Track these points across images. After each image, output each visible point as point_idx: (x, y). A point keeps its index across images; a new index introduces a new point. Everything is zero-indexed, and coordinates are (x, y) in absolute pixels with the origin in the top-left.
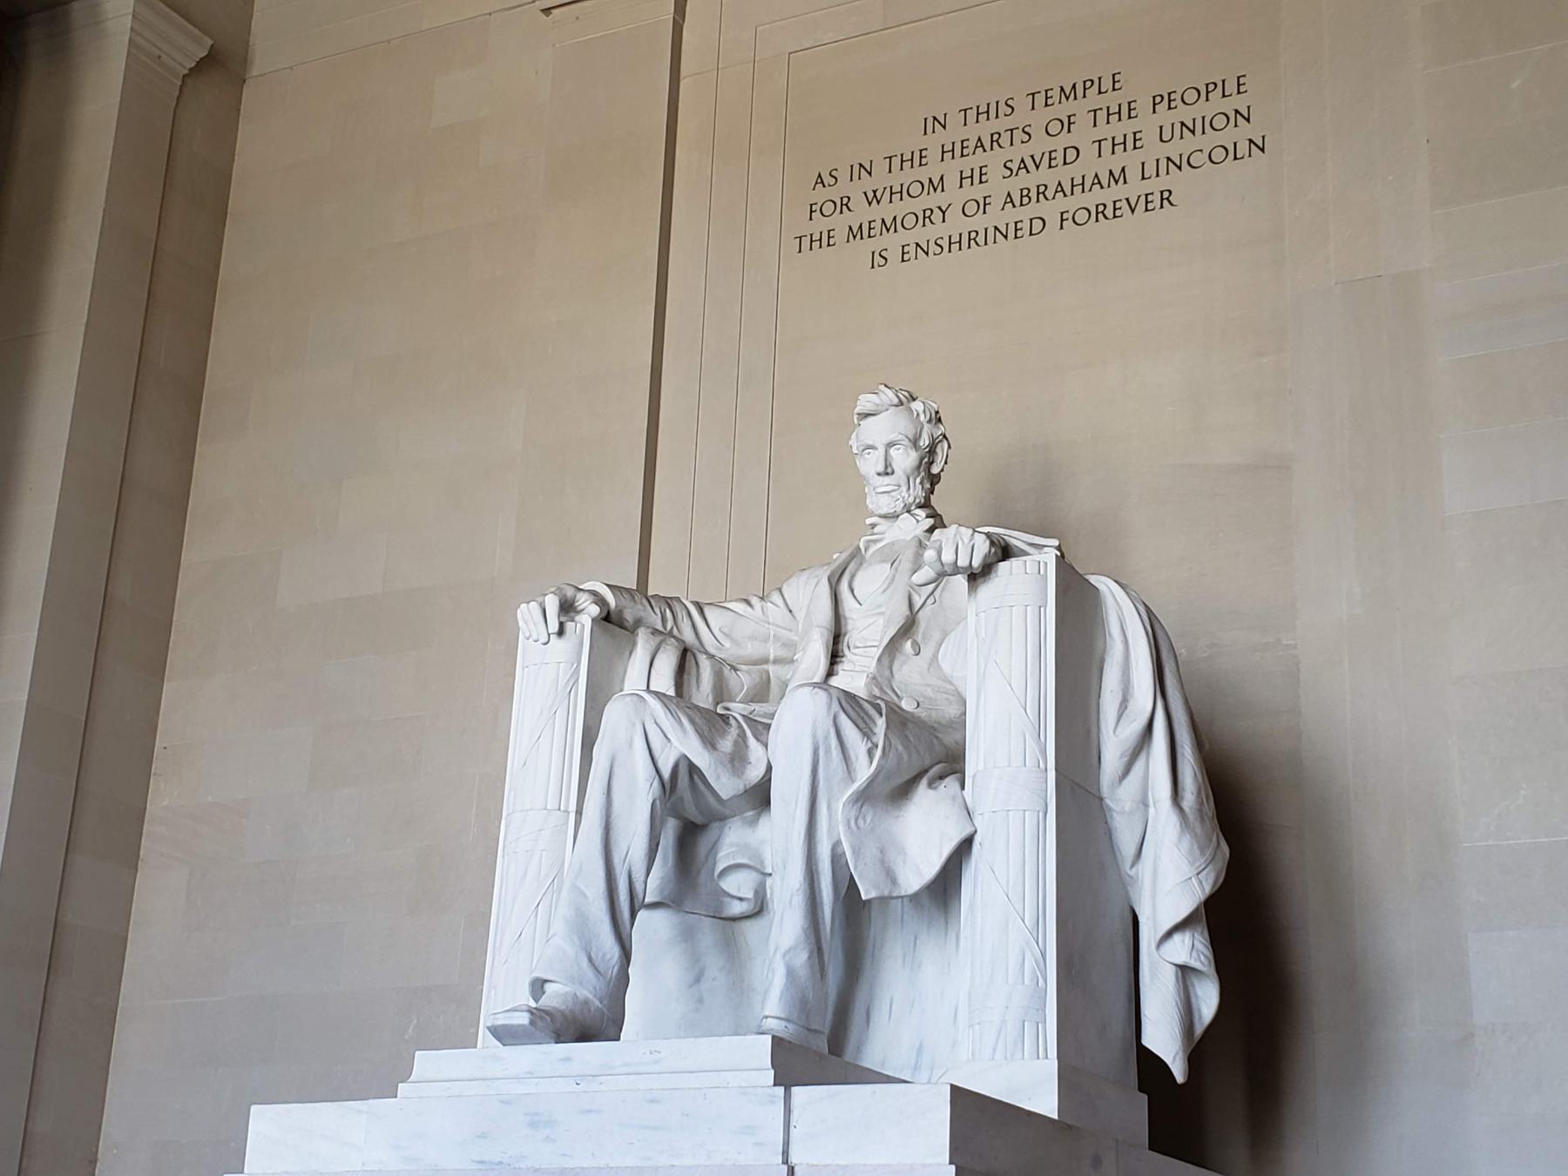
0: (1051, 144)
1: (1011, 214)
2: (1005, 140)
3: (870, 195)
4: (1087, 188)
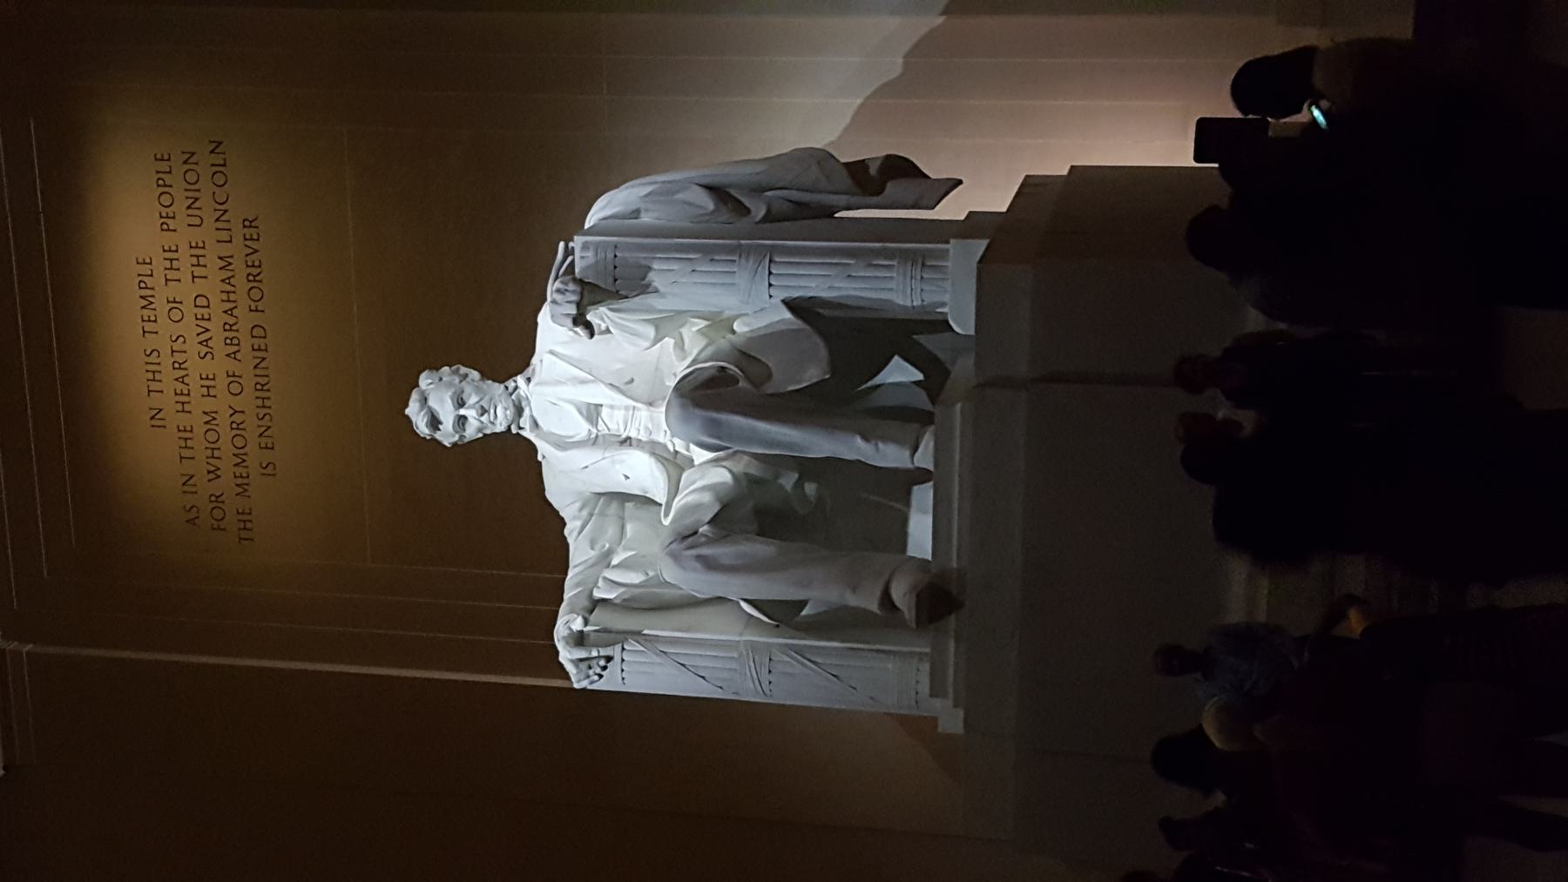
0: (189, 318)
2: (179, 358)
3: (212, 476)
4: (229, 288)
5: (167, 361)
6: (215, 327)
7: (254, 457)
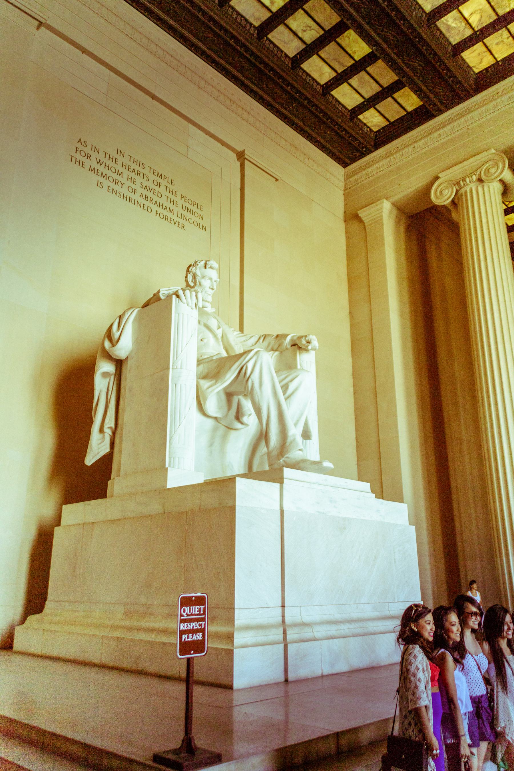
0: (154, 187)
1: (141, 201)
2: (141, 175)
3: (98, 161)
4: (164, 208)
6: (150, 195)
7: (106, 183)
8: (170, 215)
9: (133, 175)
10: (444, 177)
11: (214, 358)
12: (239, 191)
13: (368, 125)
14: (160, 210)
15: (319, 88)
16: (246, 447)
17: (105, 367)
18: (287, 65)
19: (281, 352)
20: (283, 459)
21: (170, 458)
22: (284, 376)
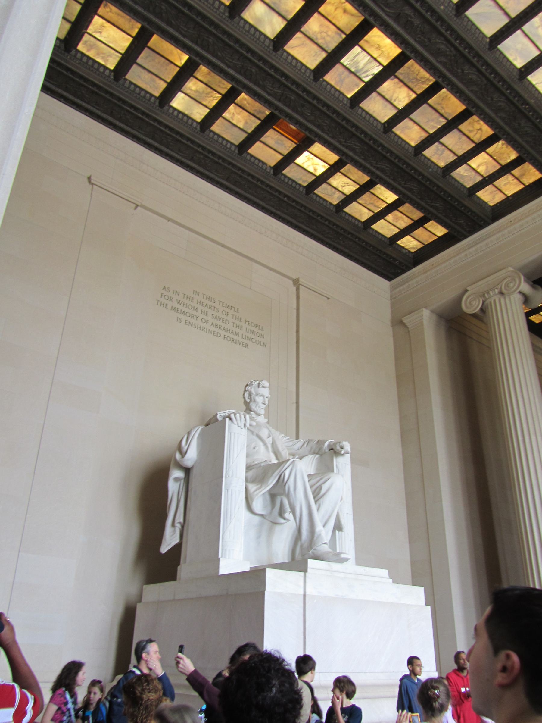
0: (223, 317)
1: (212, 329)
2: (213, 308)
5: (211, 303)
7: (184, 318)
8: (235, 337)
9: (205, 309)
10: (472, 290)
11: (262, 465)
12: (295, 311)
13: (406, 247)
14: (227, 334)
15: (360, 225)
16: (289, 538)
17: (176, 474)
18: (332, 210)
19: (321, 455)
20: (312, 551)
21: (222, 549)
22: (318, 479)
